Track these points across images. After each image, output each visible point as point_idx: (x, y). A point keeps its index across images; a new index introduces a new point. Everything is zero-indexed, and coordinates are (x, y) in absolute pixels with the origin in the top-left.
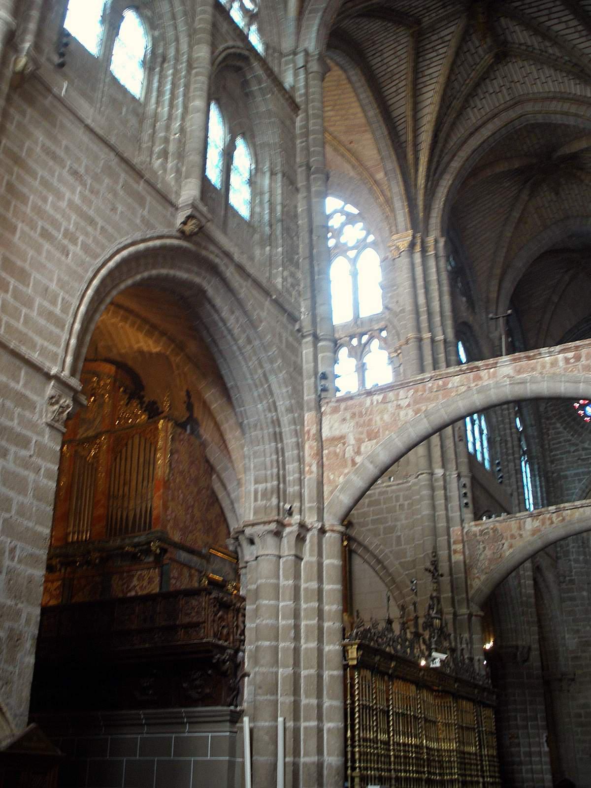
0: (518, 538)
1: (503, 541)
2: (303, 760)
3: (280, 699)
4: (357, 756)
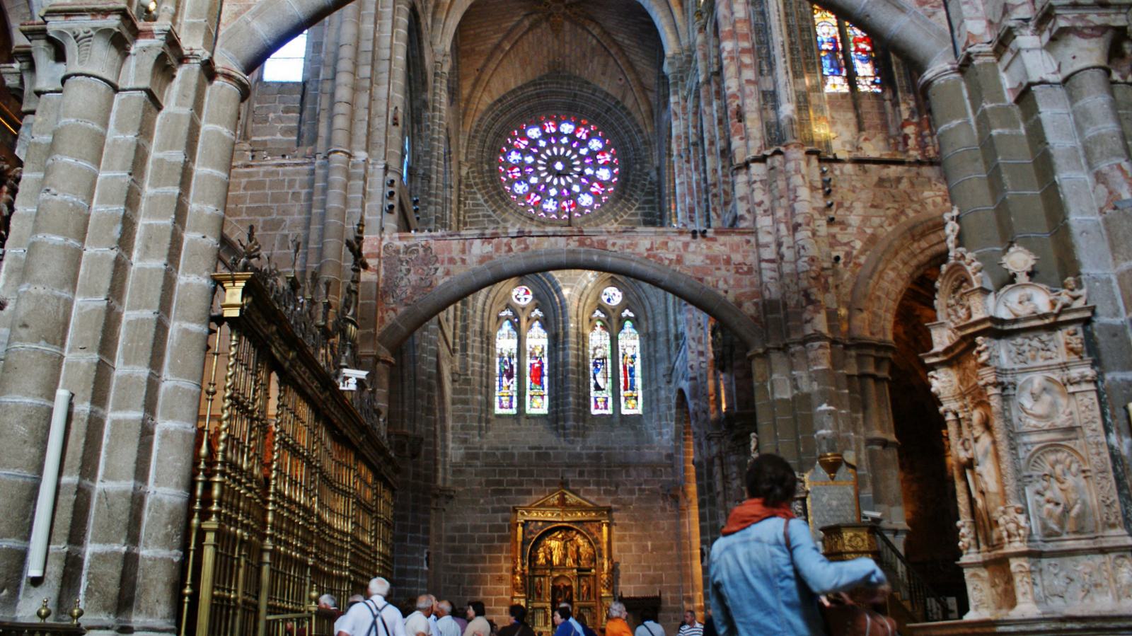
0: (459, 263)
1: (437, 265)
2: (100, 486)
3: (68, 356)
4: (216, 492)
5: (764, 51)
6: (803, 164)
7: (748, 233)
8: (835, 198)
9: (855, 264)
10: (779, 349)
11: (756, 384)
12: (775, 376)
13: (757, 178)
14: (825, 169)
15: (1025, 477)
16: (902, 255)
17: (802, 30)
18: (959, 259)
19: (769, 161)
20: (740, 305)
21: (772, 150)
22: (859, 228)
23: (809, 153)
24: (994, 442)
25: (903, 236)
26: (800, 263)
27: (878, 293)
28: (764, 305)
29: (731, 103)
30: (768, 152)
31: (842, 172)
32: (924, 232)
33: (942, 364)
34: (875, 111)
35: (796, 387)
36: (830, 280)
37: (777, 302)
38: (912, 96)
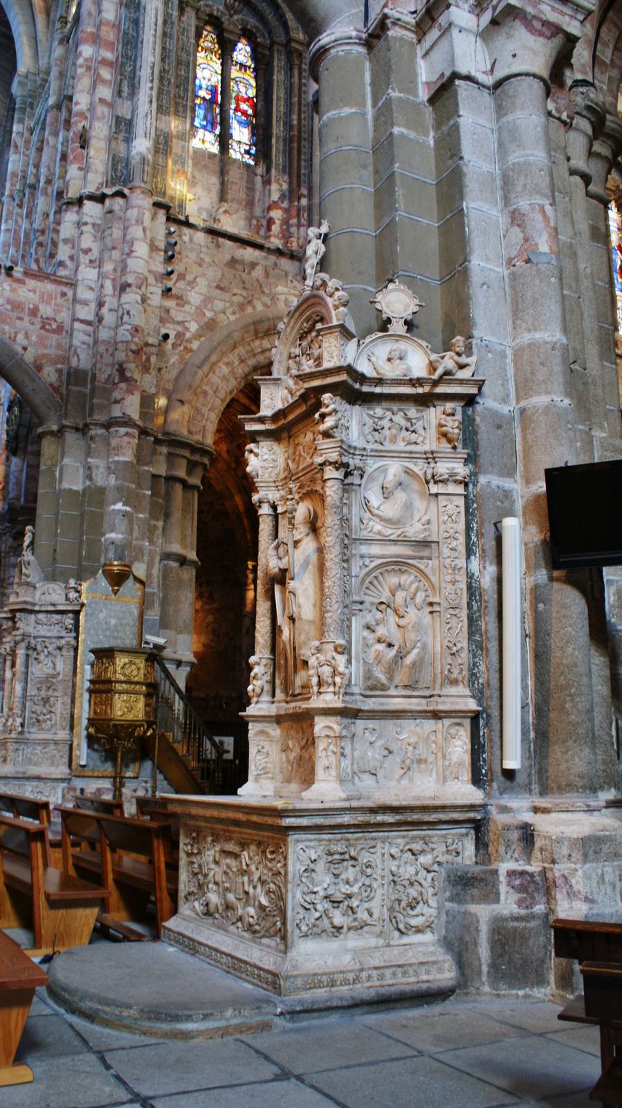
5: (129, 69)
6: (147, 216)
7: (67, 284)
8: (178, 267)
9: (186, 348)
10: (77, 429)
11: (42, 467)
12: (66, 461)
13: (89, 220)
14: (172, 229)
15: (354, 602)
16: (241, 350)
17: (179, 63)
18: (318, 289)
19: (108, 202)
20: (39, 368)
21: (114, 189)
22: (197, 308)
23: (157, 205)
24: (320, 551)
25: (245, 328)
26: (121, 330)
27: (205, 388)
28: (69, 374)
29: (76, 123)
30: (109, 191)
31: (191, 240)
32: (268, 330)
33: (268, 434)
34: (244, 183)
35: (90, 477)
36: (153, 359)
37: (85, 373)
38: (286, 177)
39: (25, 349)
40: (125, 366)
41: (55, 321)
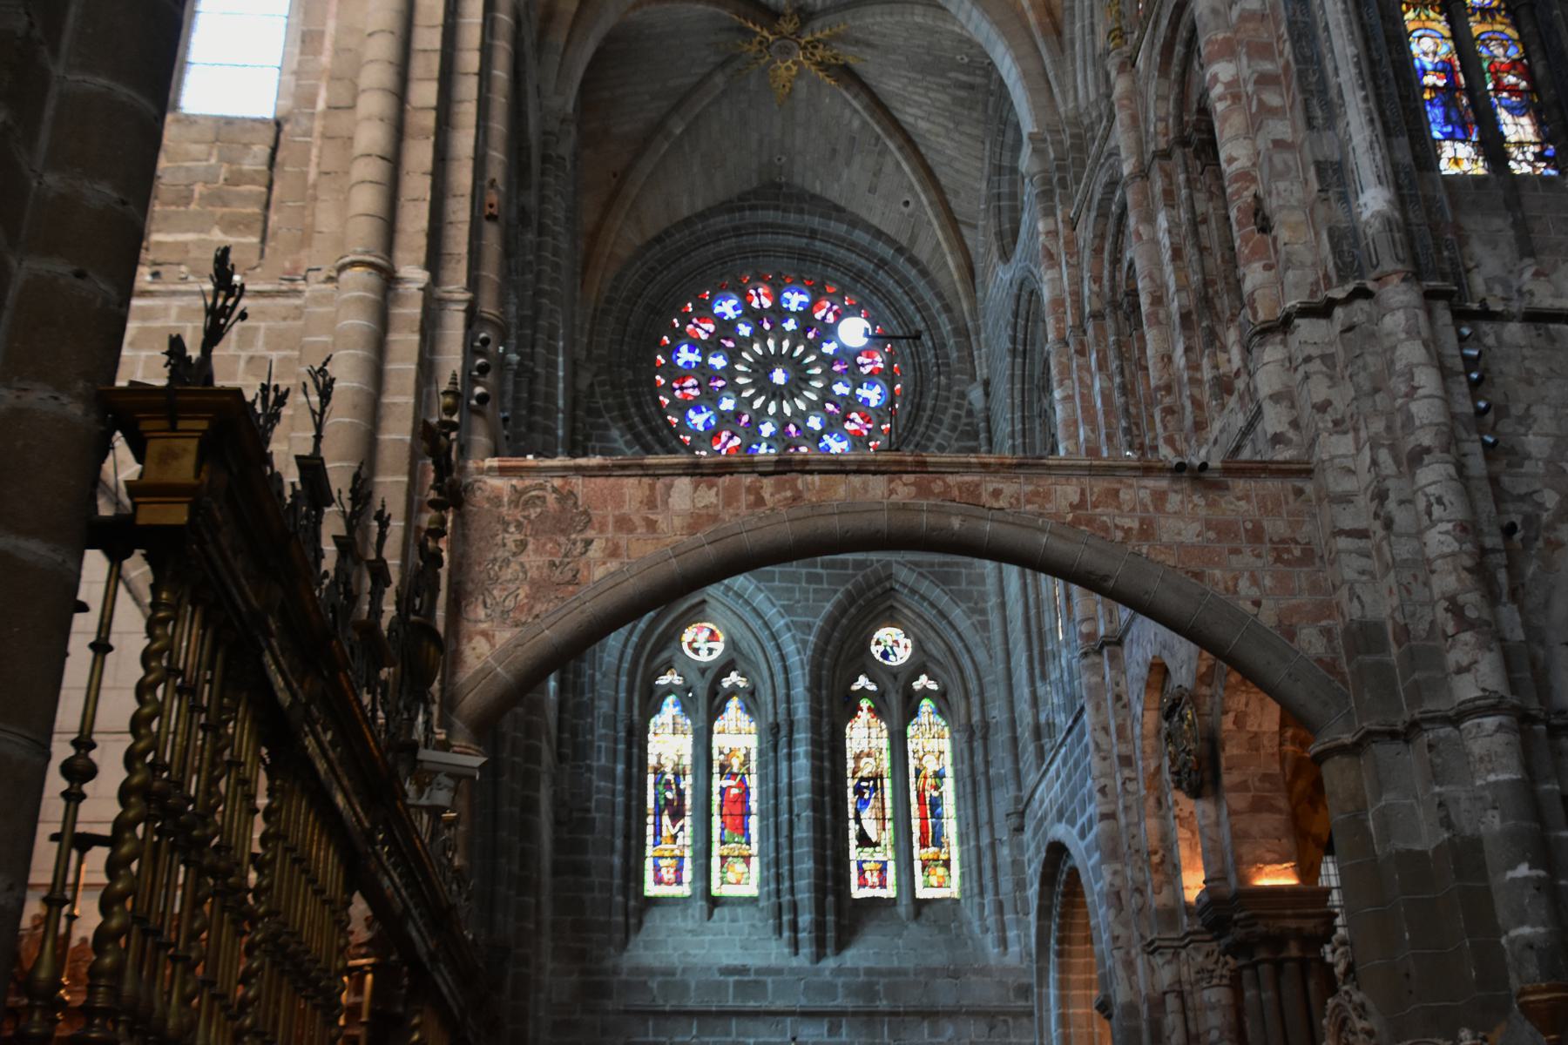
1: (590, 534)
10: (1393, 735)
13: (1314, 352)
19: (1339, 312)
20: (1291, 634)
21: (1350, 287)
22: (1549, 461)
23: (1430, 295)
37: (1379, 626)
39: (1257, 603)
40: (1461, 599)
41: (1297, 543)
